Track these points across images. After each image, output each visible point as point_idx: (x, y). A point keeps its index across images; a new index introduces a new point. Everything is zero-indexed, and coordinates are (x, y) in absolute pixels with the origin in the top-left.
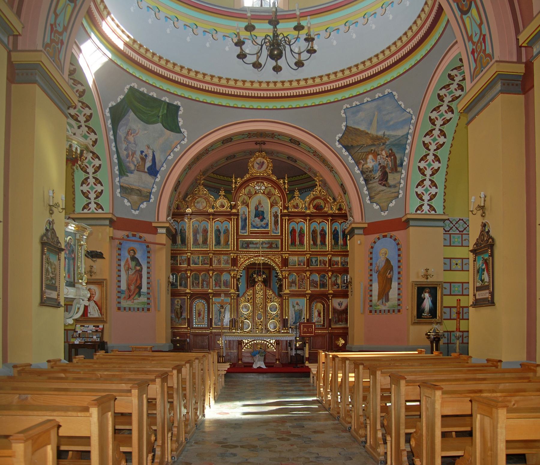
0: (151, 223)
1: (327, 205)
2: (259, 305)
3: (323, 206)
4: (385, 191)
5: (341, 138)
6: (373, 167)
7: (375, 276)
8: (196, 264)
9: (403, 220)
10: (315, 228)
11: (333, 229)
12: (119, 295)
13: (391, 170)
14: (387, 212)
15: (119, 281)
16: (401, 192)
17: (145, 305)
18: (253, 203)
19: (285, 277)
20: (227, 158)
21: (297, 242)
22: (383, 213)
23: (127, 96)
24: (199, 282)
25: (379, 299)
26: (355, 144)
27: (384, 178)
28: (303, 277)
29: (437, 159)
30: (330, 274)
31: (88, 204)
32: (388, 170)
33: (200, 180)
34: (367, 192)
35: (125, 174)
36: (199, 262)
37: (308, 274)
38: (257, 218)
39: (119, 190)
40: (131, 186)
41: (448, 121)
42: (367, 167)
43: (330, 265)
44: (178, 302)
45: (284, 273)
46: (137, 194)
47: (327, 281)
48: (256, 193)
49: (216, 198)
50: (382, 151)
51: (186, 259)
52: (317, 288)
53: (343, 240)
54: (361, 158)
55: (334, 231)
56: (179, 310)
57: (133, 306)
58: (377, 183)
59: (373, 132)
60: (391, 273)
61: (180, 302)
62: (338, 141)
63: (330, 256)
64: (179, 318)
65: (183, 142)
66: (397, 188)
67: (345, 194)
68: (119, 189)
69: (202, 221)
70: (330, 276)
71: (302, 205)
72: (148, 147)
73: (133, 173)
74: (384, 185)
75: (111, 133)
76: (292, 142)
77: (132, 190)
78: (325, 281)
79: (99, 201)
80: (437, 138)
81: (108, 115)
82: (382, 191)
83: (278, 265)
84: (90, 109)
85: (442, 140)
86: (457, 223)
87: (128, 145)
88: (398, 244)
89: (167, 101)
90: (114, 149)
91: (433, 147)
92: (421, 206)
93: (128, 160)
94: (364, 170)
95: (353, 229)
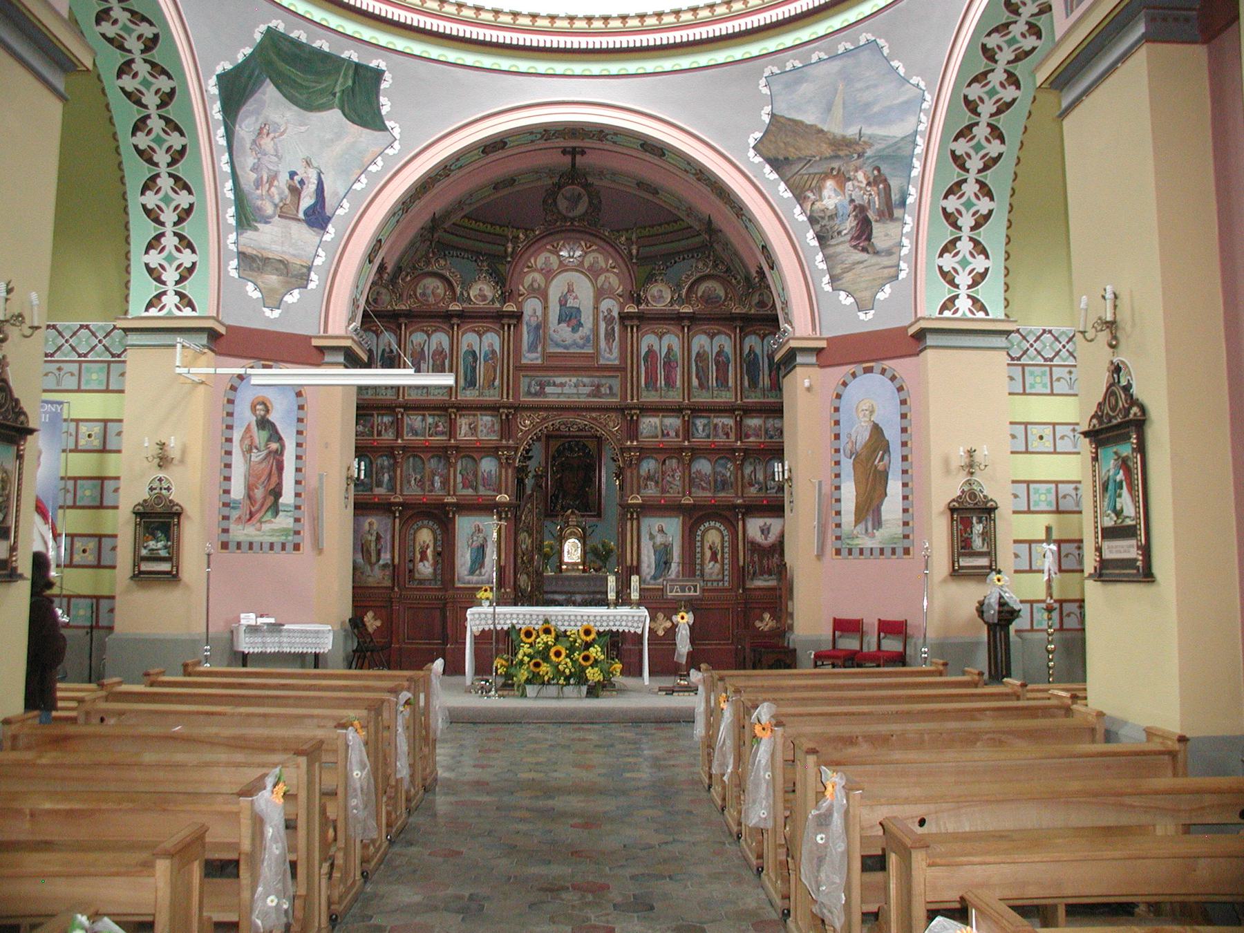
4: (865, 264)
7: (847, 465)
8: (416, 434)
9: (911, 331)
11: (746, 351)
12: (226, 511)
13: (879, 215)
14: (872, 312)
15: (228, 479)
16: (903, 265)
17: (287, 535)
20: (497, 187)
21: (661, 382)
22: (862, 315)
23: (260, 49)
25: (857, 522)
26: (792, 153)
27: (864, 232)
29: (985, 190)
31: (159, 297)
32: (871, 215)
34: (823, 266)
35: (249, 225)
38: (563, 325)
39: (234, 263)
40: (263, 252)
41: (1009, 105)
43: (739, 437)
44: (370, 524)
46: (277, 270)
50: (857, 171)
51: (392, 423)
53: (770, 375)
54: (807, 186)
56: (373, 545)
57: (261, 539)
58: (847, 245)
59: (835, 127)
60: (886, 457)
65: (390, 151)
66: (895, 257)
68: (236, 260)
72: (308, 163)
73: (269, 222)
74: (864, 250)
75: (221, 131)
76: (646, 151)
77: (266, 260)
79: (187, 288)
80: (984, 143)
81: (214, 91)
82: (859, 263)
84: (170, 77)
85: (994, 148)
86: (1038, 338)
87: (259, 159)
88: (900, 389)
89: (355, 58)
90: (227, 168)
91: (974, 164)
92: (953, 299)
93: (259, 192)
94: (815, 215)
95: (792, 354)
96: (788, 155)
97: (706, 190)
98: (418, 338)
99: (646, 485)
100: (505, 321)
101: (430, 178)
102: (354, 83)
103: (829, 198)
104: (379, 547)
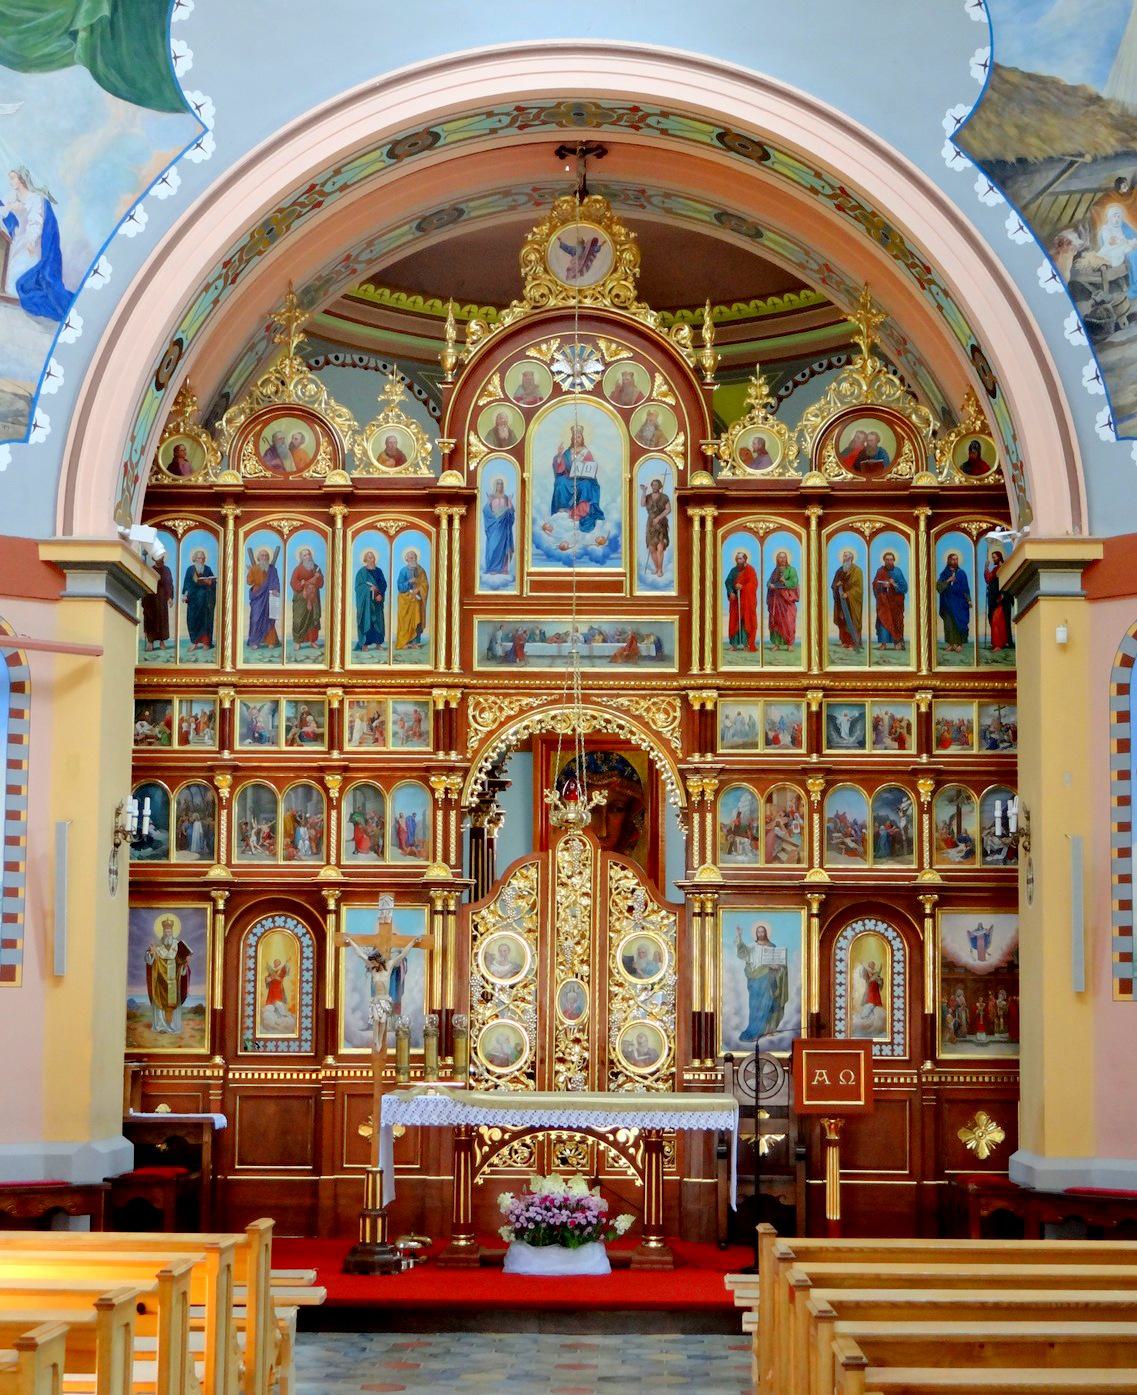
0: (34, 545)
1: (907, 447)
2: (570, 943)
3: (891, 453)
5: (967, 125)
6: (1126, 262)
8: (260, 739)
10: (849, 558)
11: (941, 566)
18: (545, 439)
19: (702, 802)
21: (763, 632)
24: (273, 829)
26: (1035, 150)
28: (790, 804)
30: (925, 786)
33: (286, 330)
34: (1097, 388)
36: (276, 728)
37: (816, 784)
38: (563, 515)
42: (1096, 264)
43: (925, 746)
44: (166, 925)
45: (694, 782)
47: (910, 820)
48: (557, 390)
49: (366, 415)
51: (211, 717)
52: (863, 856)
53: (990, 616)
55: (945, 575)
56: (171, 967)
61: (176, 930)
62: (955, 139)
63: (924, 697)
64: (169, 1009)
65: (195, 156)
67: (992, 393)
69: (294, 530)
70: (925, 798)
71: (786, 447)
72: (24, 182)
76: (730, 149)
78: (902, 823)
83: (666, 743)
94: (1082, 279)
95: (1030, 572)
96: (1023, 152)
97: (856, 231)
98: (264, 542)
99: (733, 844)
100: (442, 510)
101: (280, 211)
102: (114, 9)
103: (1113, 242)
104: (183, 972)
